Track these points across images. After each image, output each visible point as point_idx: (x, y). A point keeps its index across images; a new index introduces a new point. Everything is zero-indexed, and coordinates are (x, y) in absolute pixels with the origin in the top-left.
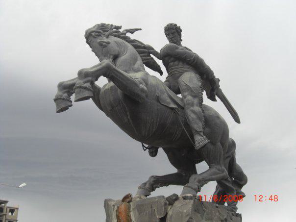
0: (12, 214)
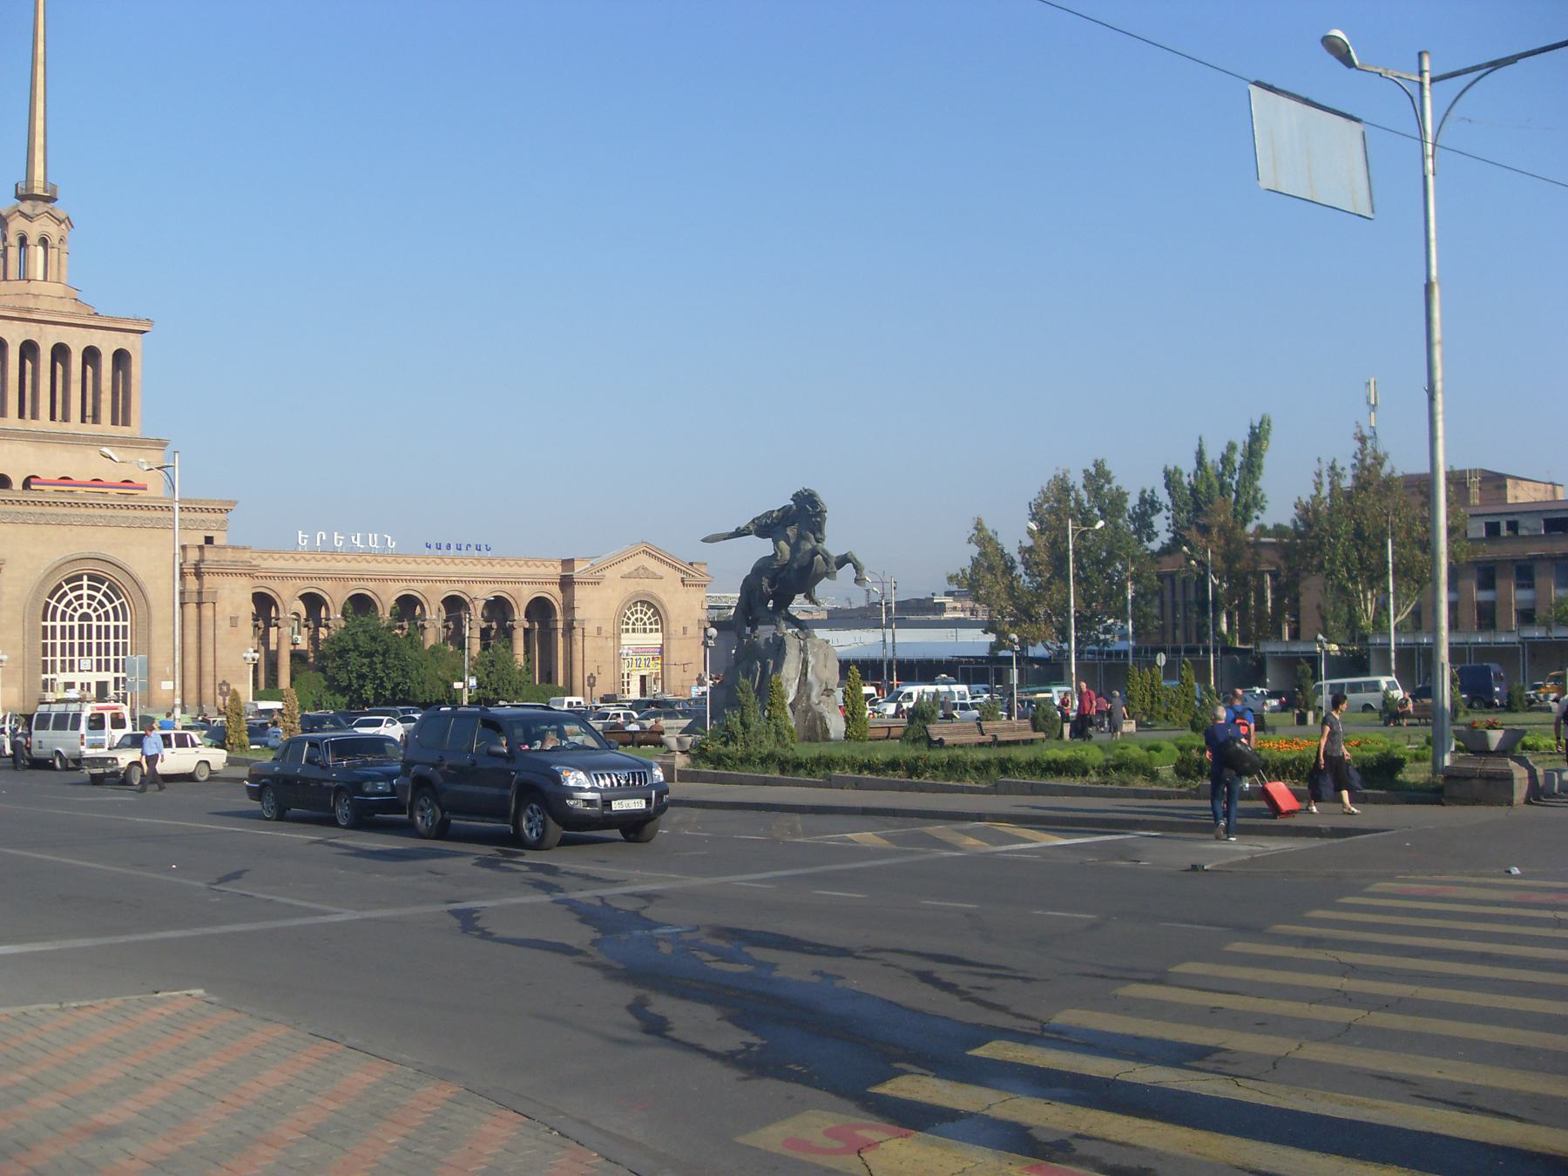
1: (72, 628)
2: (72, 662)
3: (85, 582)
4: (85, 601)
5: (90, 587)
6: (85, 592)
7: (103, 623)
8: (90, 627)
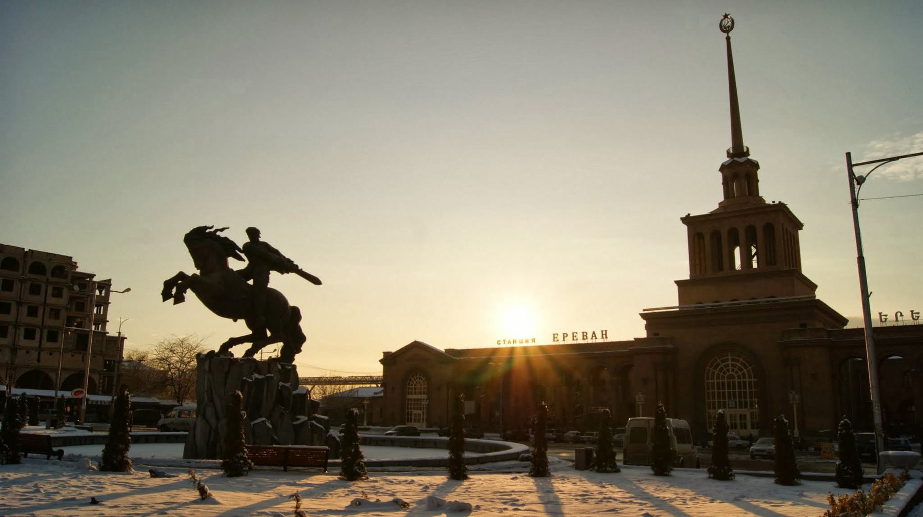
0: (101, 292)
1: (723, 383)
2: (725, 403)
3: (730, 357)
4: (730, 368)
5: (733, 360)
6: (730, 362)
7: (742, 380)
8: (734, 382)
